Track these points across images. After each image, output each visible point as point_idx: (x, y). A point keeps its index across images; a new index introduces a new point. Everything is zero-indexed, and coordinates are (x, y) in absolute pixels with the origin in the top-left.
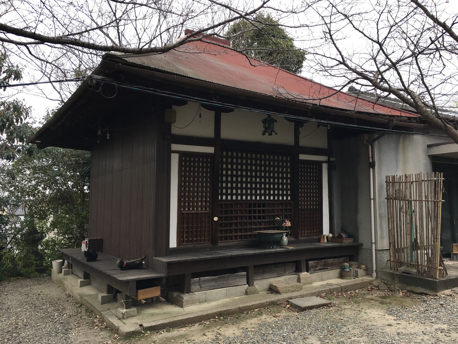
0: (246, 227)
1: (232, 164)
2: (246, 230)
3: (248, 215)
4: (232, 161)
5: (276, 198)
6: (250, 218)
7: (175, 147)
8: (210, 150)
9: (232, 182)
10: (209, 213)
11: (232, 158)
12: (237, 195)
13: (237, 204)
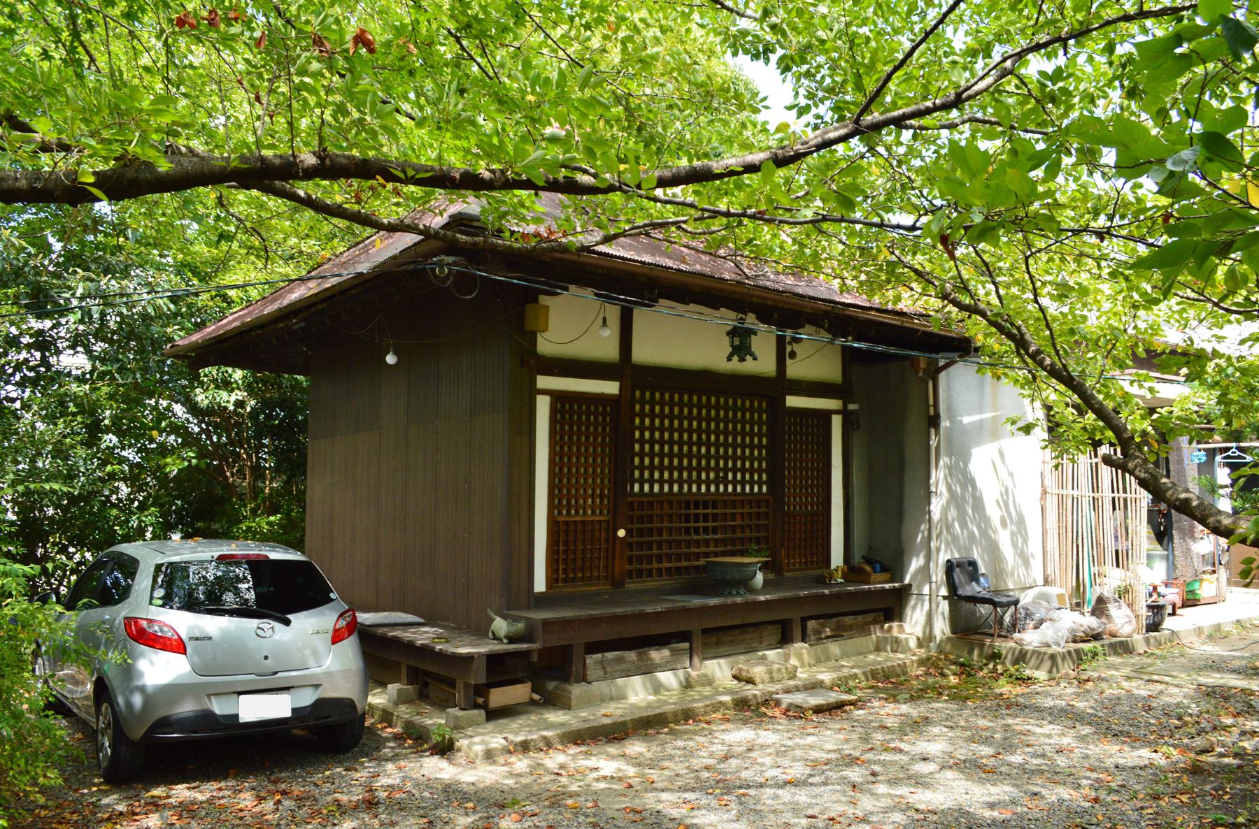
0: (680, 551)
1: (652, 416)
2: (679, 557)
3: (683, 525)
4: (652, 410)
5: (739, 489)
6: (687, 531)
7: (543, 382)
8: (610, 388)
9: (652, 455)
10: (607, 522)
11: (653, 403)
12: (661, 482)
13: (662, 503)
